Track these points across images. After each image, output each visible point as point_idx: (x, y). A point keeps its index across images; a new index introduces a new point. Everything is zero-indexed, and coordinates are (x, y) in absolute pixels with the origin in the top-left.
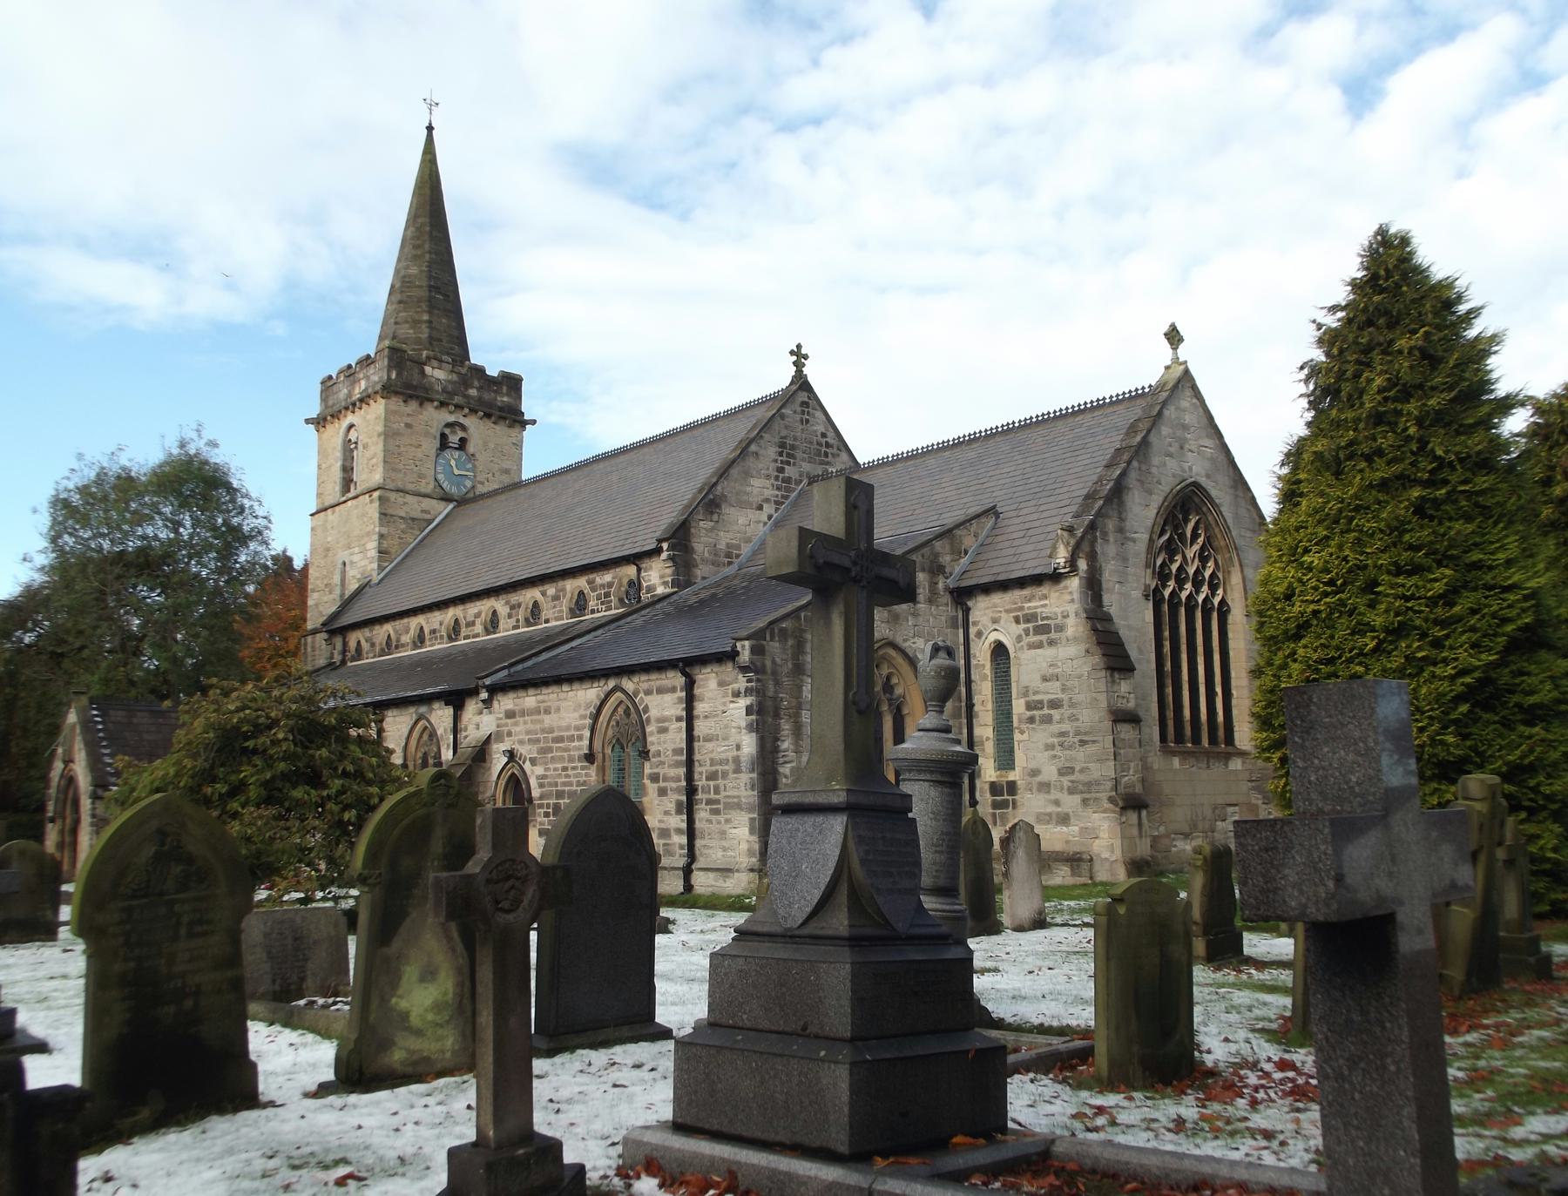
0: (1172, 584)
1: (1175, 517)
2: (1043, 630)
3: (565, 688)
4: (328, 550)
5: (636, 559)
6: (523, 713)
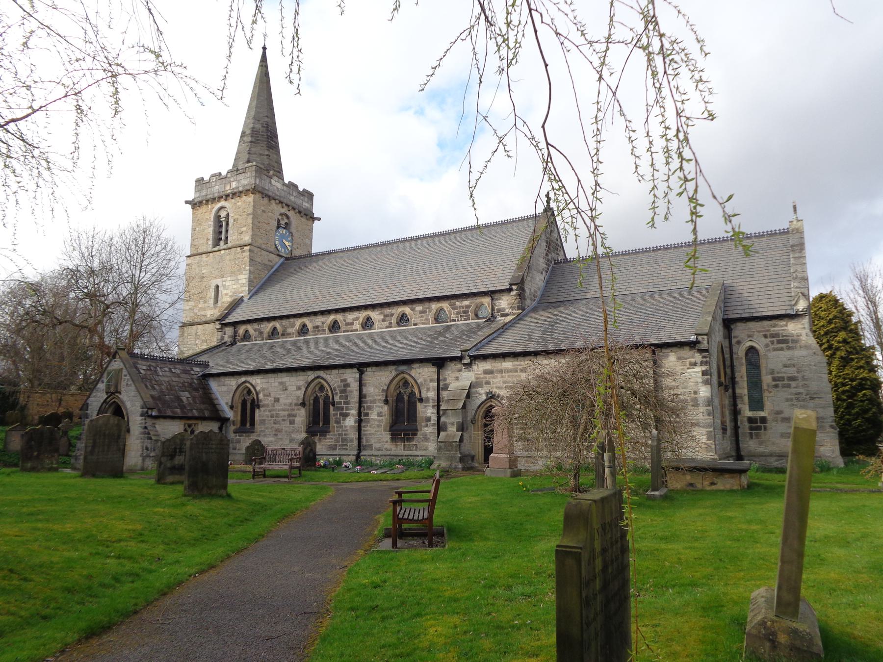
4: (203, 277)
5: (492, 294)
6: (501, 371)
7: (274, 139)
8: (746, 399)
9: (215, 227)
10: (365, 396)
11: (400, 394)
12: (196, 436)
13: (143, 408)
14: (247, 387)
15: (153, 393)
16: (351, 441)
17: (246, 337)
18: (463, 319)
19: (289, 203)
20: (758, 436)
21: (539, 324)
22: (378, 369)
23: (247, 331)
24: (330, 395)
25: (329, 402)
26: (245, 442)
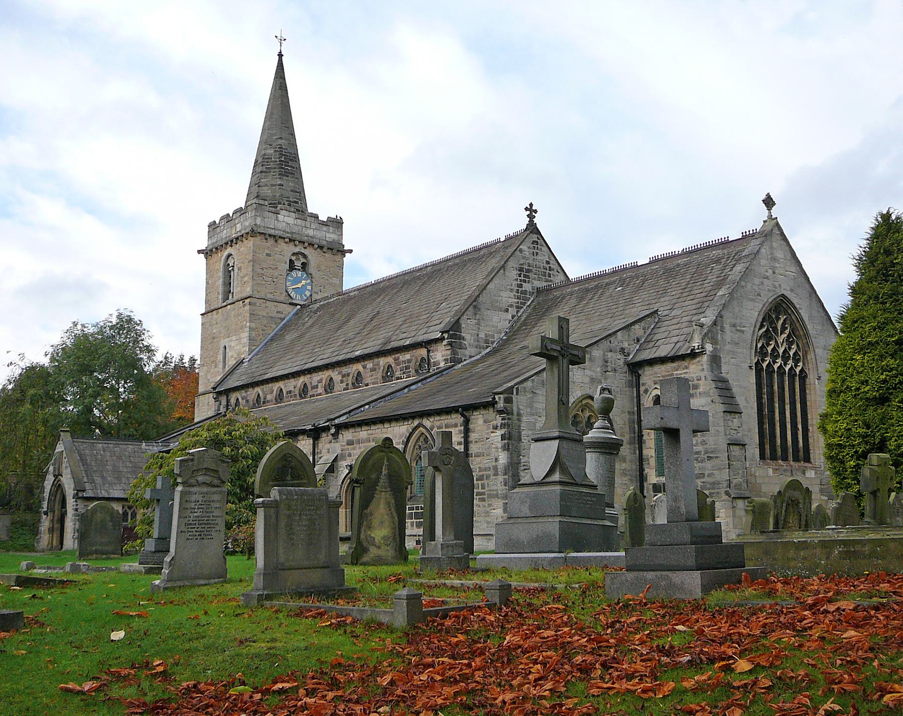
0: (768, 359)
1: (770, 316)
3: (386, 425)
5: (428, 344)
6: (359, 442)
9: (224, 278)
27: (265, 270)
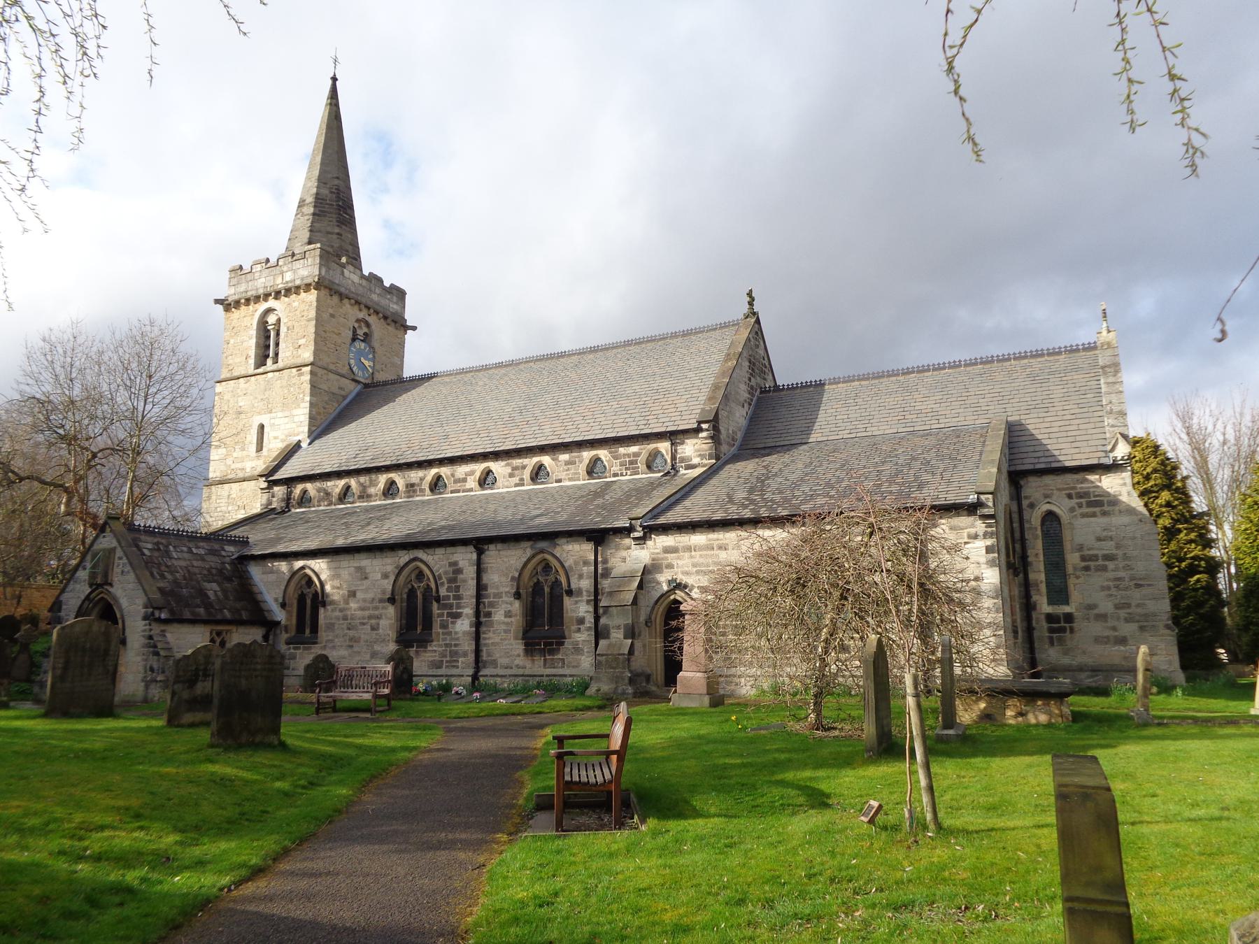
2: (1098, 504)
4: (240, 413)
6: (689, 549)
7: (349, 211)
8: (1043, 587)
10: (485, 588)
11: (538, 584)
12: (230, 650)
13: (146, 607)
14: (306, 575)
15: (161, 585)
16: (465, 654)
17: (304, 500)
18: (629, 473)
19: (370, 304)
20: (1061, 641)
21: (742, 480)
22: (505, 546)
23: (305, 492)
24: (433, 586)
25: (431, 596)
26: (302, 659)
27: (328, 334)
